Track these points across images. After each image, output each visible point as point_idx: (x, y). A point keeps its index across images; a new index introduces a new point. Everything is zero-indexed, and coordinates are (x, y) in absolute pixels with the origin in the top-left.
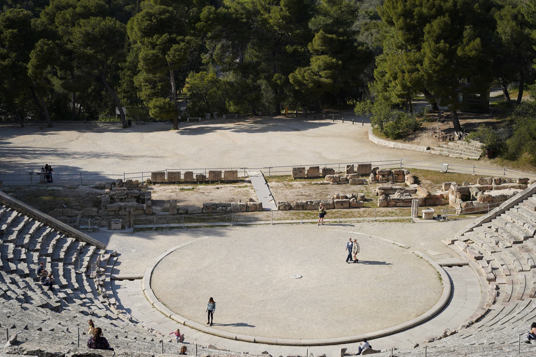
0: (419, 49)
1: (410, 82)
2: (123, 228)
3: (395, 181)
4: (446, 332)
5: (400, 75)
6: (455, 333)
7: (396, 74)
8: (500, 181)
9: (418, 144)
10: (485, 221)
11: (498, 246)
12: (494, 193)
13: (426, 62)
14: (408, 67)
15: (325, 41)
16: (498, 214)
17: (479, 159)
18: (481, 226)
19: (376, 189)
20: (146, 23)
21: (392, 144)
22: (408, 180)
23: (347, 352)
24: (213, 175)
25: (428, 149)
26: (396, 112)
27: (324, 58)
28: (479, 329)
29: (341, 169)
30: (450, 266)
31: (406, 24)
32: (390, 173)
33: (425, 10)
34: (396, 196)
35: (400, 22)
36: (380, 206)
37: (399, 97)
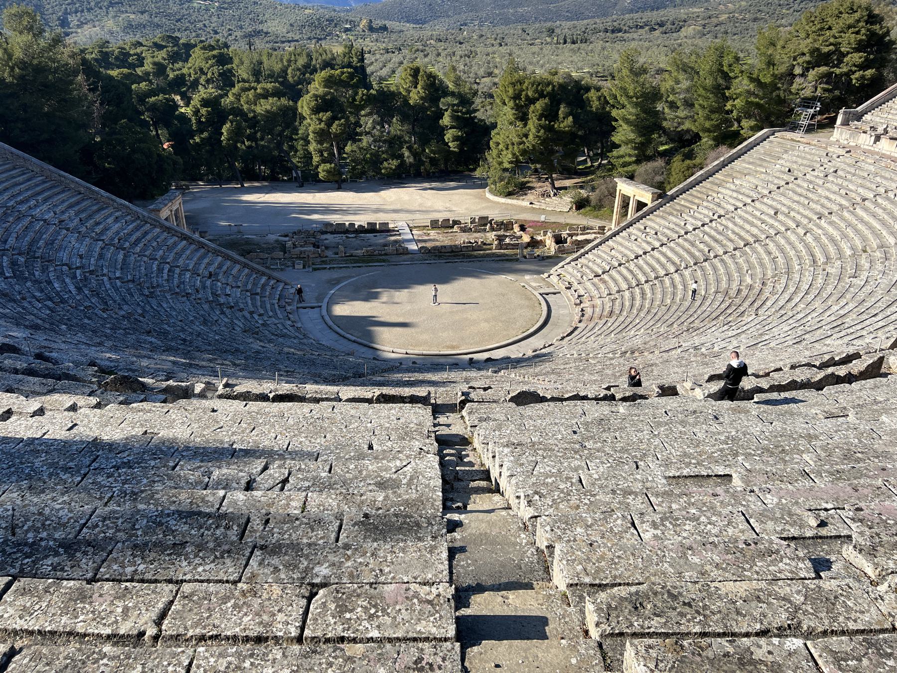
0: (525, 125)
2: (304, 267)
3: (506, 230)
5: (510, 147)
8: (584, 229)
10: (573, 260)
12: (580, 238)
15: (454, 118)
16: (583, 255)
19: (491, 236)
20: (313, 104)
21: (503, 200)
22: (516, 228)
25: (531, 203)
26: (507, 174)
29: (466, 220)
31: (516, 105)
32: (502, 223)
33: (530, 94)
34: (507, 240)
35: (511, 104)
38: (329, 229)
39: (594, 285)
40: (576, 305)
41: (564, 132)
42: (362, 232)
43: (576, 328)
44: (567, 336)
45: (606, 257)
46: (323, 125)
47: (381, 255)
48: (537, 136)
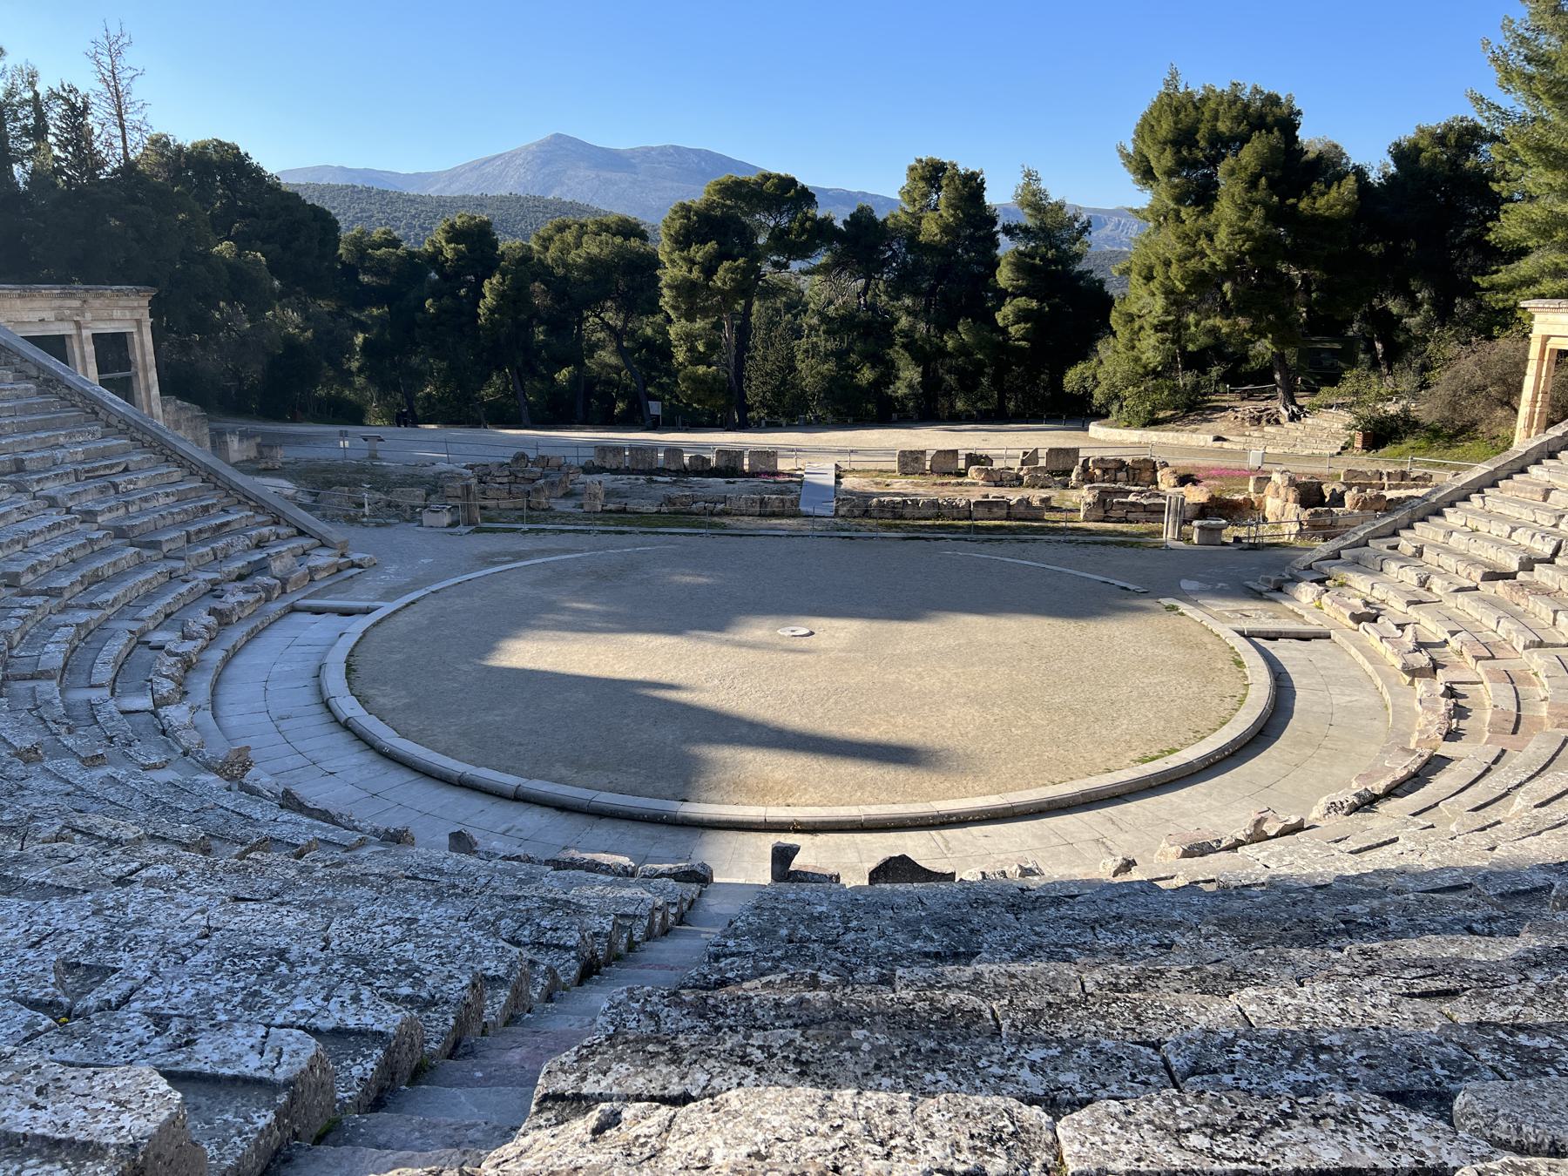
1: (1183, 279)
4: (1259, 822)
5: (1159, 271)
6: (1298, 828)
7: (1151, 268)
9: (1194, 431)
11: (1429, 589)
13: (1222, 235)
14: (1180, 248)
17: (1339, 454)
18: (1366, 545)
20: (677, 224)
22: (1166, 482)
23: (797, 863)
24: (725, 458)
25: (1218, 439)
27: (1022, 302)
28: (1422, 821)
30: (1273, 637)
33: (1223, 126)
36: (1086, 519)
37: (1157, 331)
38: (611, 462)
39: (1493, 603)
40: (1413, 672)
41: (1328, 222)
42: (698, 473)
43: (1435, 764)
44: (1392, 792)
45: (1526, 515)
46: (695, 274)
47: (712, 514)
48: (1242, 231)
